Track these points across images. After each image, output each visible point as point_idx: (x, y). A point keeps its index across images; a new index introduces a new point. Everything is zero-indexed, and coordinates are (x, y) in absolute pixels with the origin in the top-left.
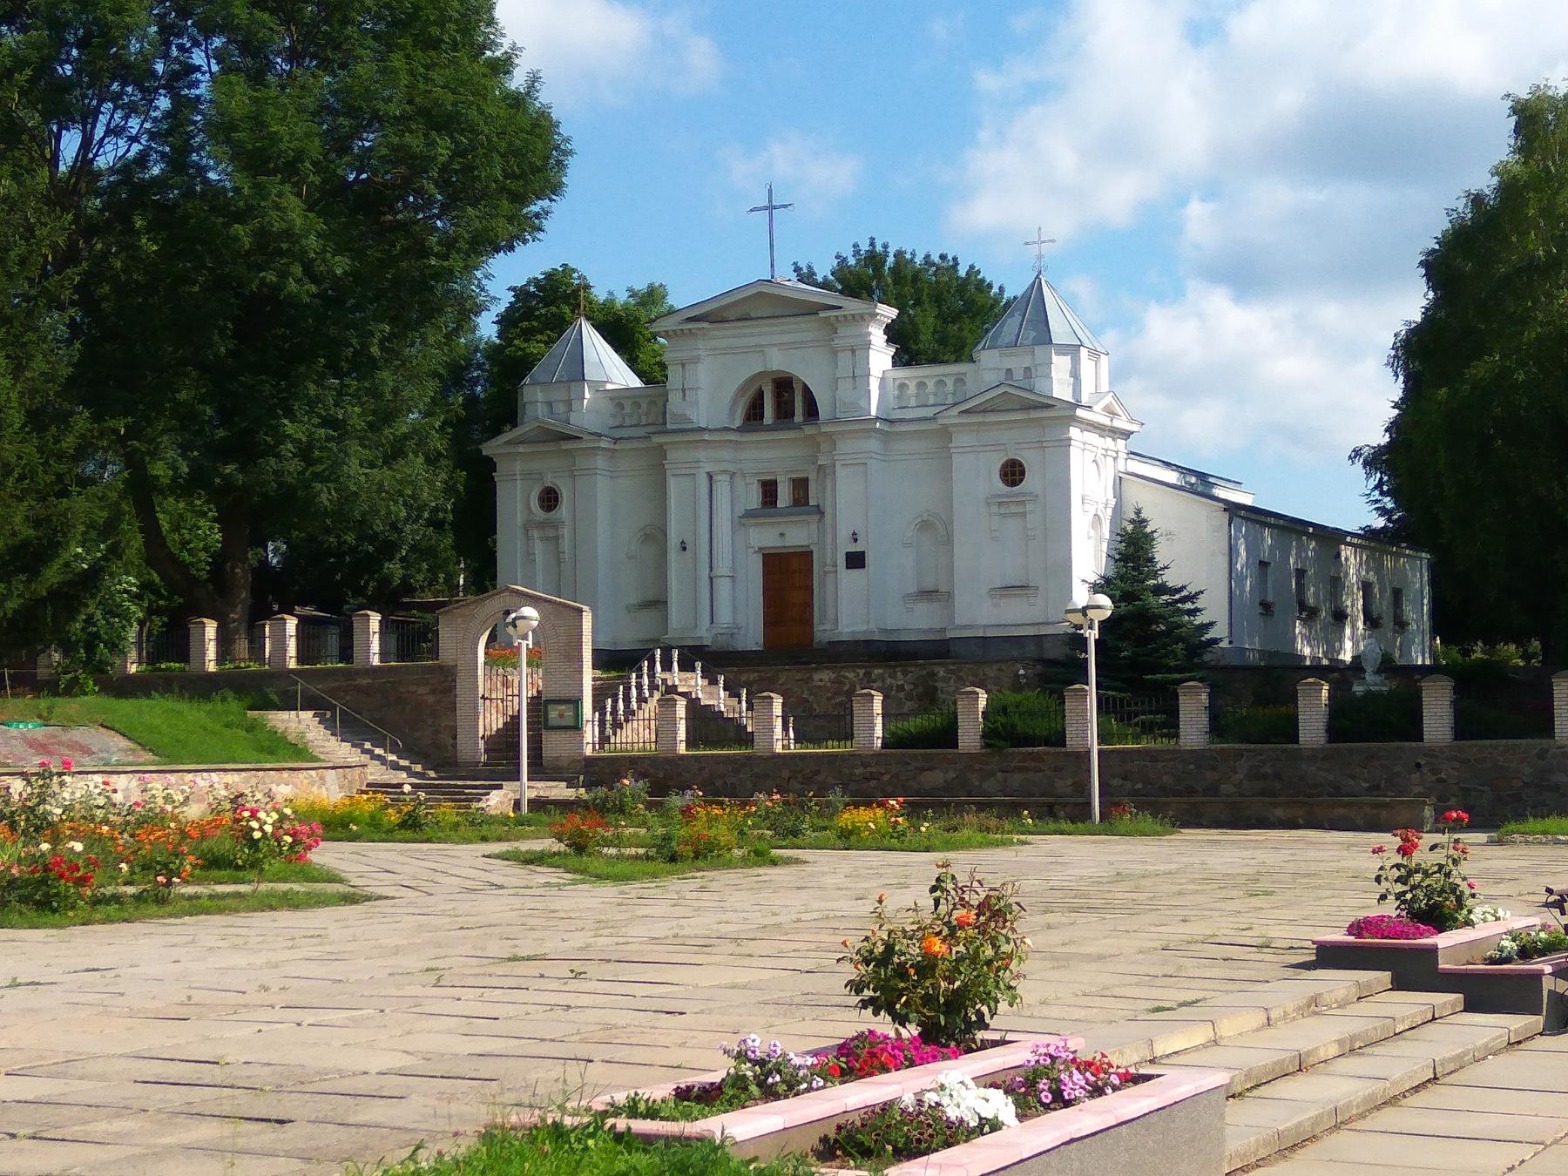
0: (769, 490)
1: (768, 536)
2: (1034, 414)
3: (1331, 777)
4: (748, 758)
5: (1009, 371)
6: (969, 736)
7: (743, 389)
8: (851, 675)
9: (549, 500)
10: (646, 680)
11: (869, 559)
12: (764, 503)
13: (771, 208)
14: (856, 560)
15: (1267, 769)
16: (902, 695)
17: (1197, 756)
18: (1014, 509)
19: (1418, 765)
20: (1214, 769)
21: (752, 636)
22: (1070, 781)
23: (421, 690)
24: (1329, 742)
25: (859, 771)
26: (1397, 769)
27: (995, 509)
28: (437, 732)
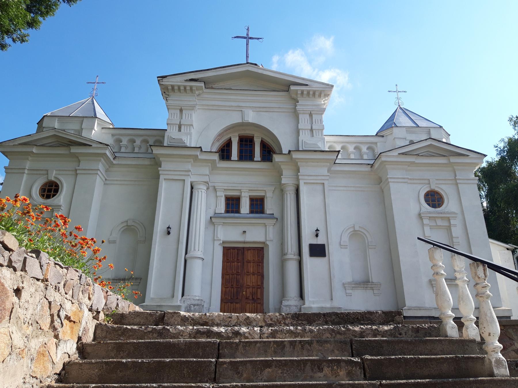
0: (233, 204)
1: (233, 233)
2: (453, 160)
7: (220, 135)
13: (248, 38)
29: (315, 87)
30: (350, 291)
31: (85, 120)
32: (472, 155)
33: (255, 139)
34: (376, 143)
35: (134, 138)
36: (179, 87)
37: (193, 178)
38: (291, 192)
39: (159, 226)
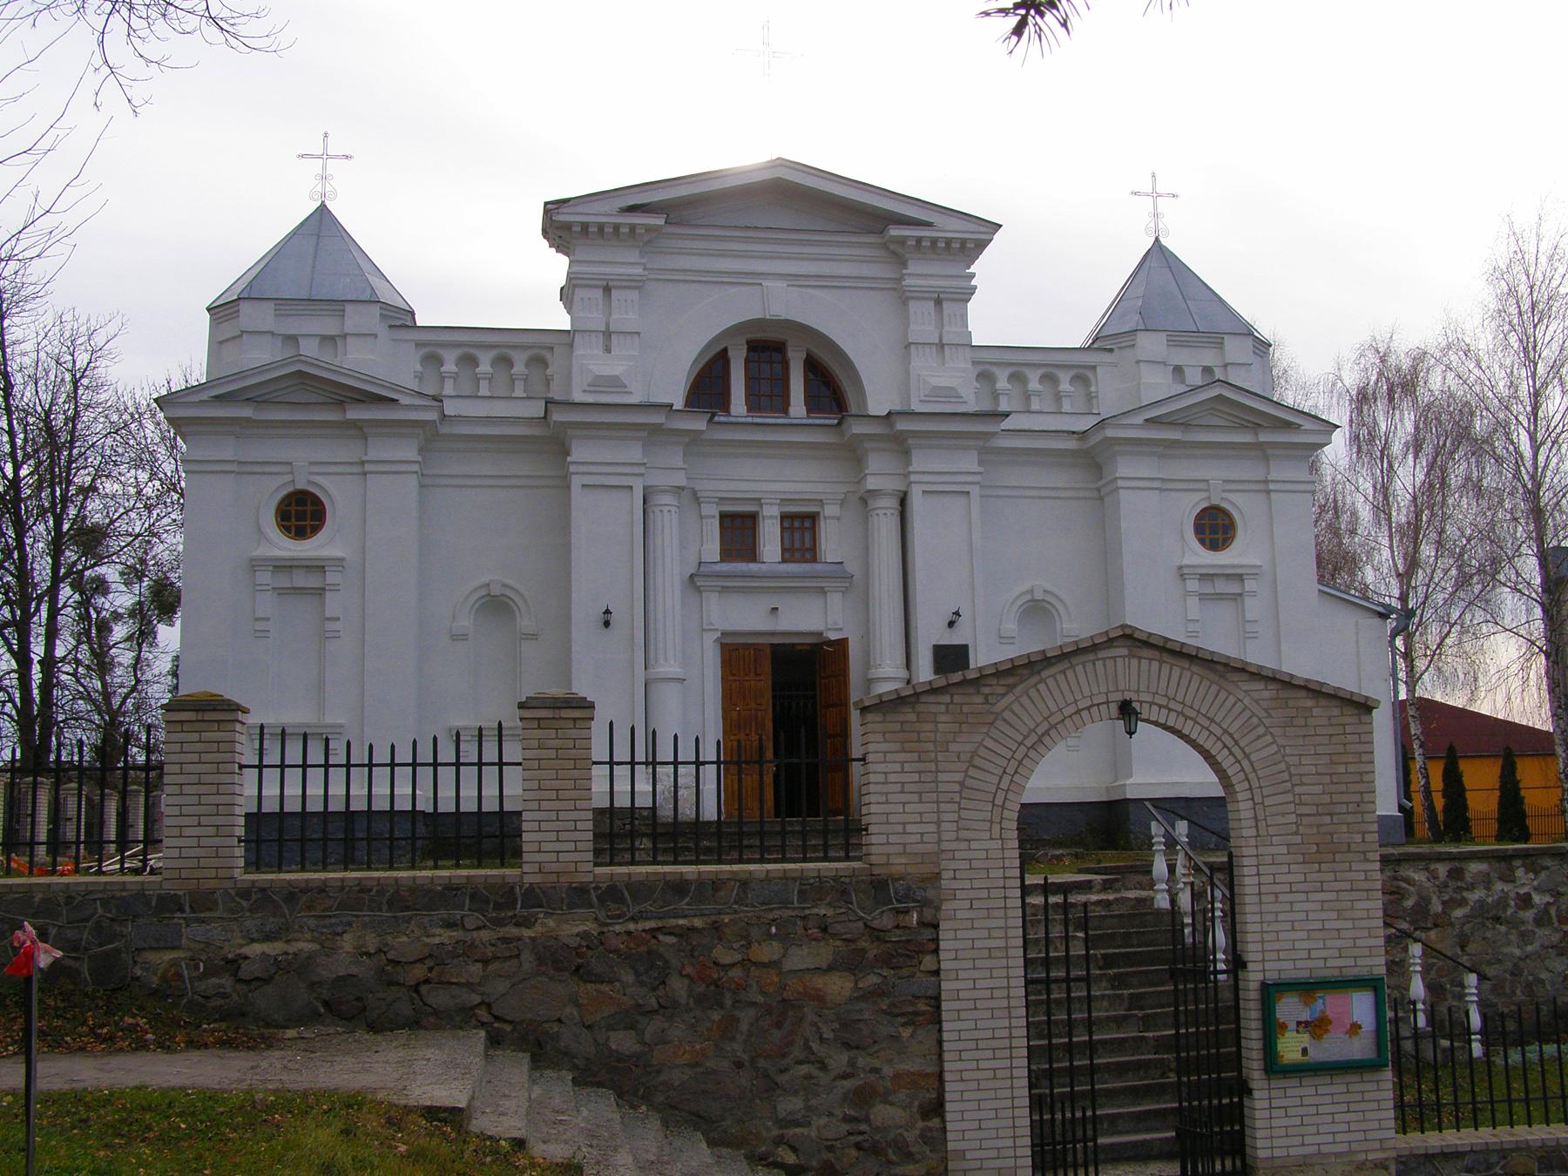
0: (739, 531)
12: (727, 554)
16: (1528, 915)
23: (800, 958)
28: (864, 1097)
29: (952, 229)
31: (349, 308)
33: (791, 354)
35: (472, 351)
36: (601, 227)
38: (889, 512)
39: (584, 614)
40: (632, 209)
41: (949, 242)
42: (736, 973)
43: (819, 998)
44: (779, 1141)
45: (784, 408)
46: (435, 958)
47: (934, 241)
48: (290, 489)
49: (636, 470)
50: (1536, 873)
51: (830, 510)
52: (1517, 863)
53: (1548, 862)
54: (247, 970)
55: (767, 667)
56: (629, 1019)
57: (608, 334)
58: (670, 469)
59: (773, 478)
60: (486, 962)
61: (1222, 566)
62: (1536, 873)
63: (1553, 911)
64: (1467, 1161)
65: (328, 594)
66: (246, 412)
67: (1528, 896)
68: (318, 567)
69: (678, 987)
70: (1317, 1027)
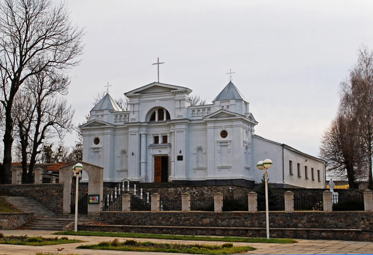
0: (156, 139)
3: (334, 222)
4: (149, 213)
5: (223, 107)
6: (218, 207)
8: (180, 189)
9: (97, 141)
10: (119, 189)
11: (184, 158)
13: (158, 64)
14: (180, 158)
15: (313, 219)
17: (290, 215)
18: (224, 144)
19: (363, 219)
20: (296, 219)
21: (151, 179)
22: (249, 222)
23: (54, 191)
24: (333, 210)
25: (183, 218)
26: (356, 219)
27: (219, 144)
28: (57, 204)
30: (195, 171)
31: (104, 110)
32: (237, 115)
34: (210, 108)
35: (121, 115)
37: (141, 133)
40: (136, 93)
41: (180, 91)
42: (49, 193)
43: (55, 195)
44: (51, 208)
45: (163, 119)
46: (29, 191)
47: (178, 92)
48: (95, 138)
49: (137, 132)
50: (196, 189)
51: (168, 135)
52: (193, 188)
53: (198, 188)
54: (17, 192)
55: (161, 160)
56: (41, 196)
57: (134, 112)
58: (143, 131)
59: (160, 131)
60: (32, 191)
61: (223, 141)
62: (196, 189)
63: (198, 195)
64: (107, 213)
65: (100, 152)
66: (89, 128)
67: (195, 192)
68: (98, 148)
69: (45, 194)
70: (93, 199)
